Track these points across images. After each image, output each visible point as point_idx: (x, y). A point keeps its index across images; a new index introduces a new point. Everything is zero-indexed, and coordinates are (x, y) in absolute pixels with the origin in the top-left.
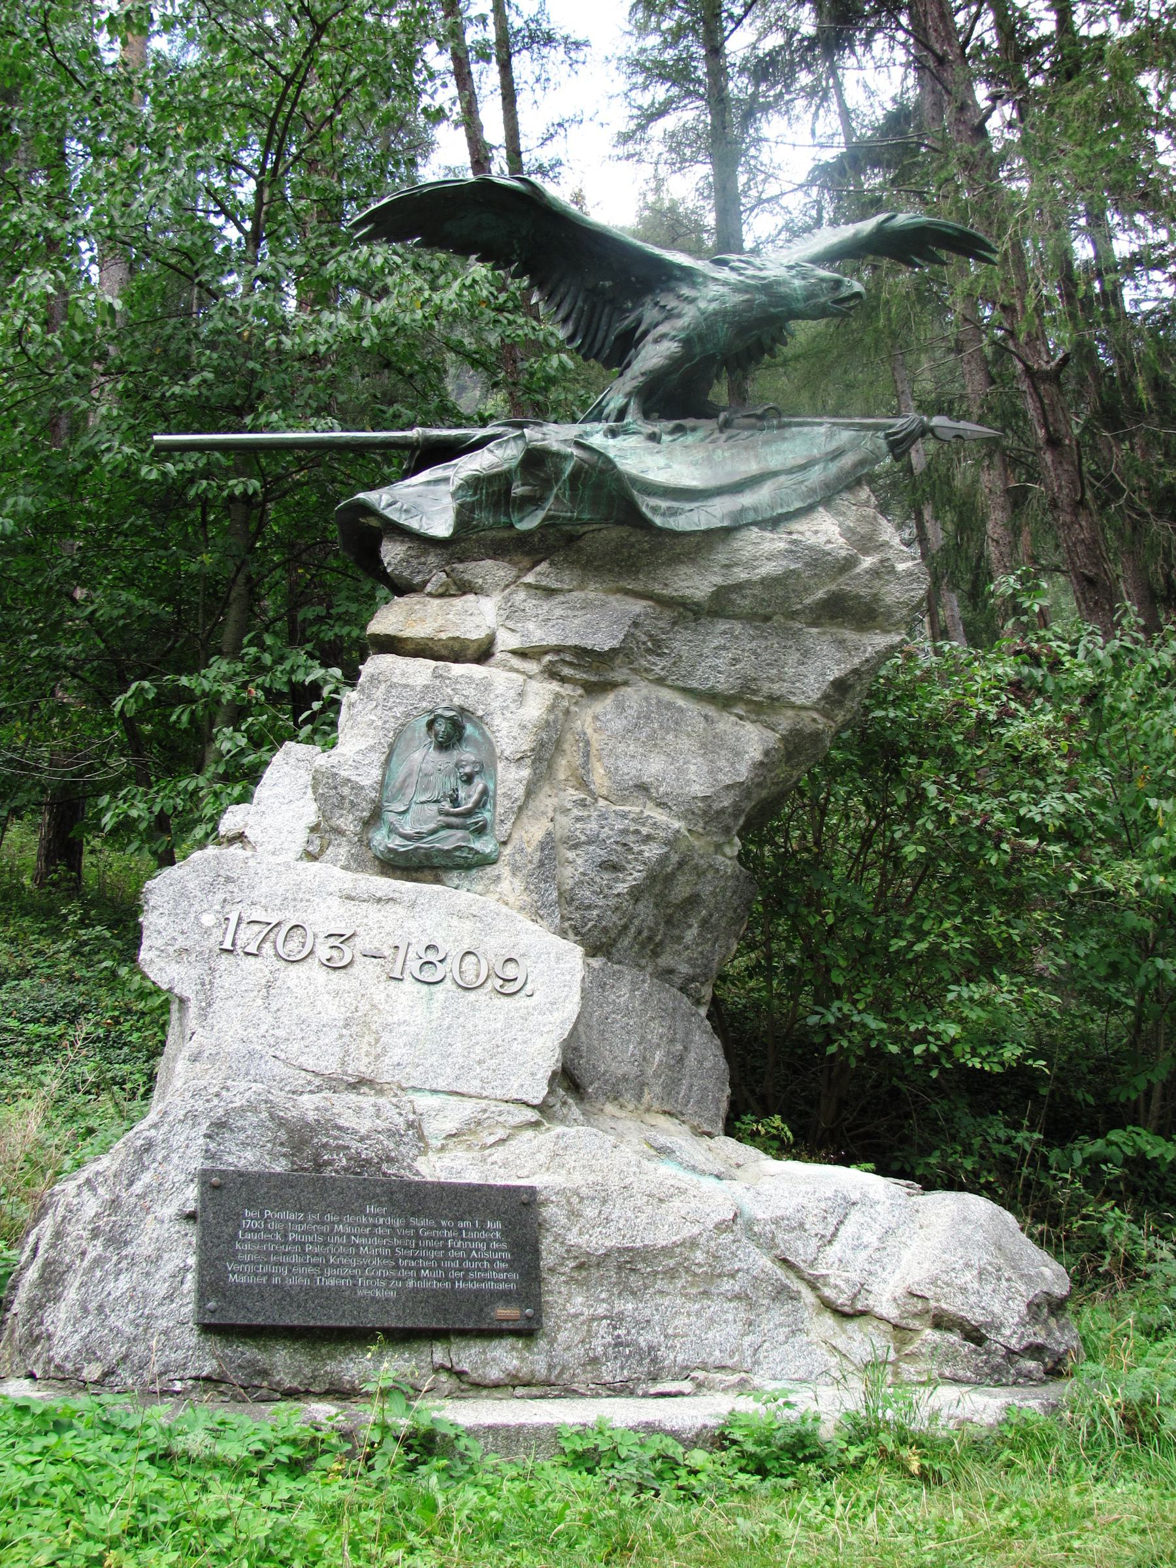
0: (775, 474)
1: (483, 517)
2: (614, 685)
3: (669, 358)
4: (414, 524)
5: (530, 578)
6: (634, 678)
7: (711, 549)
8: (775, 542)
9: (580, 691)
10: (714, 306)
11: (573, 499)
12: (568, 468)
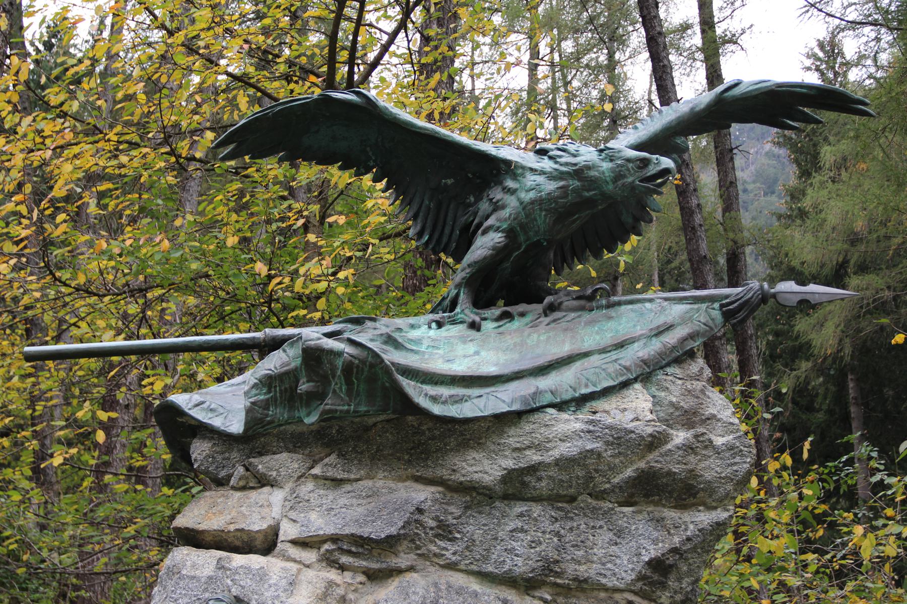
0: (586, 355)
1: (277, 413)
2: (400, 571)
3: (494, 248)
4: (217, 422)
5: (317, 471)
6: (420, 563)
7: (502, 433)
8: (570, 423)
9: (361, 578)
10: (532, 195)
11: (349, 392)
12: (339, 363)
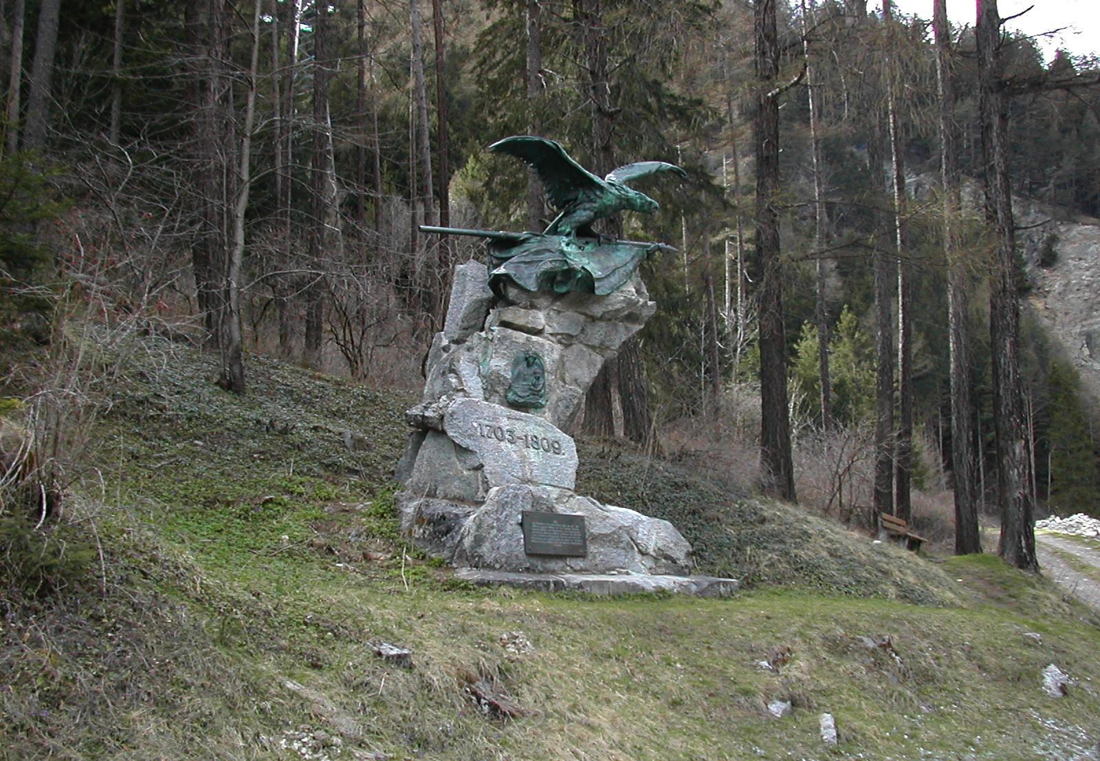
4: (521, 283)
